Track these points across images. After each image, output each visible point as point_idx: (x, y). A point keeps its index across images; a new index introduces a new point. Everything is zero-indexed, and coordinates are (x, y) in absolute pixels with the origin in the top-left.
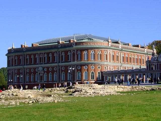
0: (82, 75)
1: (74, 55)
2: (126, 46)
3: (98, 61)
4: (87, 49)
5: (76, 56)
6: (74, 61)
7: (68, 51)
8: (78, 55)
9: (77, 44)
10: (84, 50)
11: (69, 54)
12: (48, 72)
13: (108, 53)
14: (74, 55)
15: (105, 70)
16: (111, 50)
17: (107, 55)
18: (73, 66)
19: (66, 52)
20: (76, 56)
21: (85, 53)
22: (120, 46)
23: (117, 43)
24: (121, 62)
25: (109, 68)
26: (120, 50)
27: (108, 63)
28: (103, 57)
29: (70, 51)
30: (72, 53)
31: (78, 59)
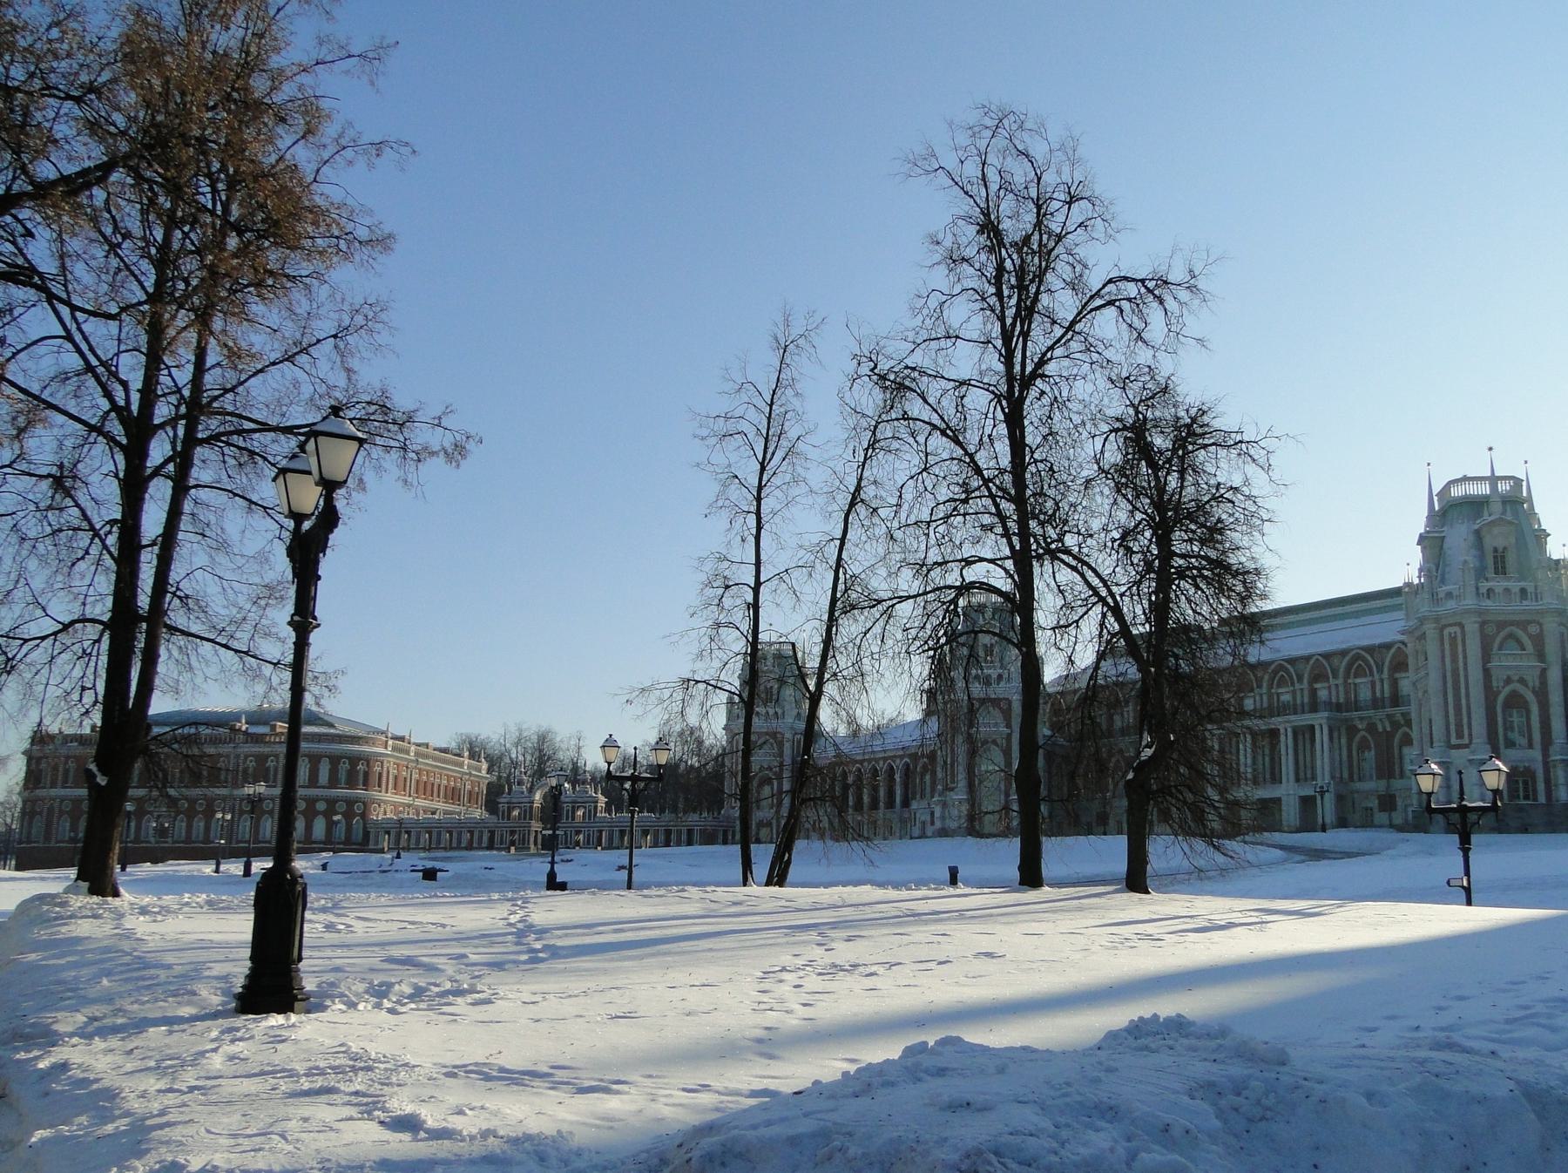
7: (267, 757)
12: (190, 815)
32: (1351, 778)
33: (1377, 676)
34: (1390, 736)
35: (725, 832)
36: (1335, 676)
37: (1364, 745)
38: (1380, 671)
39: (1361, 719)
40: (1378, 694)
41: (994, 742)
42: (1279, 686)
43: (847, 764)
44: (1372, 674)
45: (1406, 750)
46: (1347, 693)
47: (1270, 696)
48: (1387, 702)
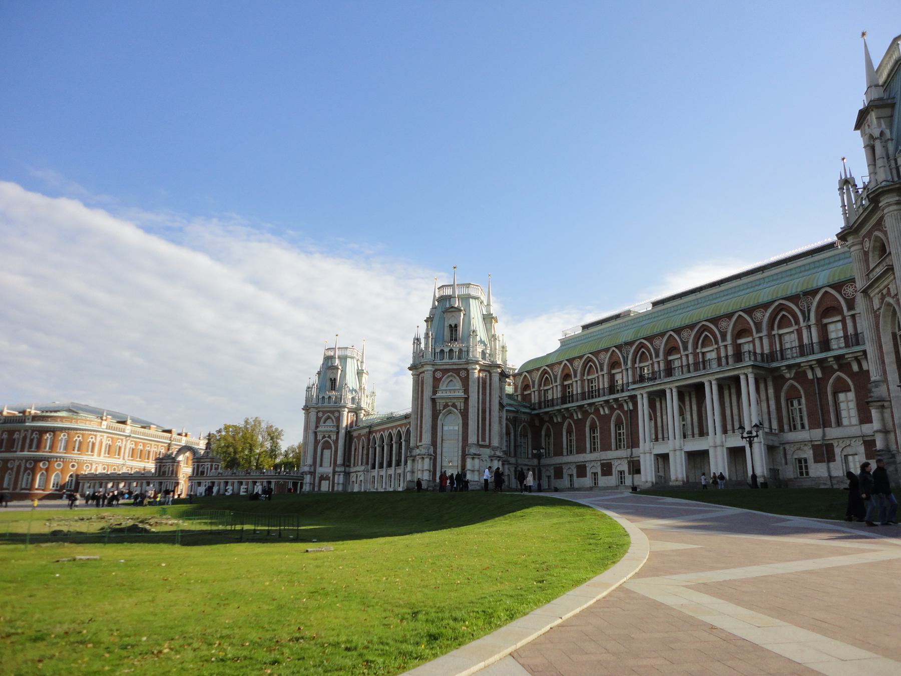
0: (33, 480)
1: (25, 438)
2: (146, 431)
3: (75, 455)
4: (54, 431)
5: (28, 441)
6: (22, 450)
7: (15, 431)
8: (32, 440)
9: (35, 418)
10: (46, 432)
11: (16, 436)
13: (98, 439)
14: (25, 438)
15: (85, 471)
16: (105, 435)
17: (93, 444)
18: (20, 459)
19: (11, 432)
20: (28, 441)
21: (48, 436)
22: (128, 429)
23: (124, 423)
24: (126, 458)
25: (94, 467)
26: (127, 436)
27: (95, 458)
28: (84, 447)
29: (19, 431)
30: (23, 435)
31: (30, 446)
32: (781, 429)
33: (802, 324)
34: (821, 383)
35: (295, 484)
36: (759, 330)
37: (793, 395)
38: (807, 318)
39: (789, 367)
40: (806, 341)
41: (454, 406)
42: (703, 346)
43: (376, 432)
44: (797, 322)
45: (842, 396)
46: (771, 344)
47: (696, 355)
48: (816, 348)
